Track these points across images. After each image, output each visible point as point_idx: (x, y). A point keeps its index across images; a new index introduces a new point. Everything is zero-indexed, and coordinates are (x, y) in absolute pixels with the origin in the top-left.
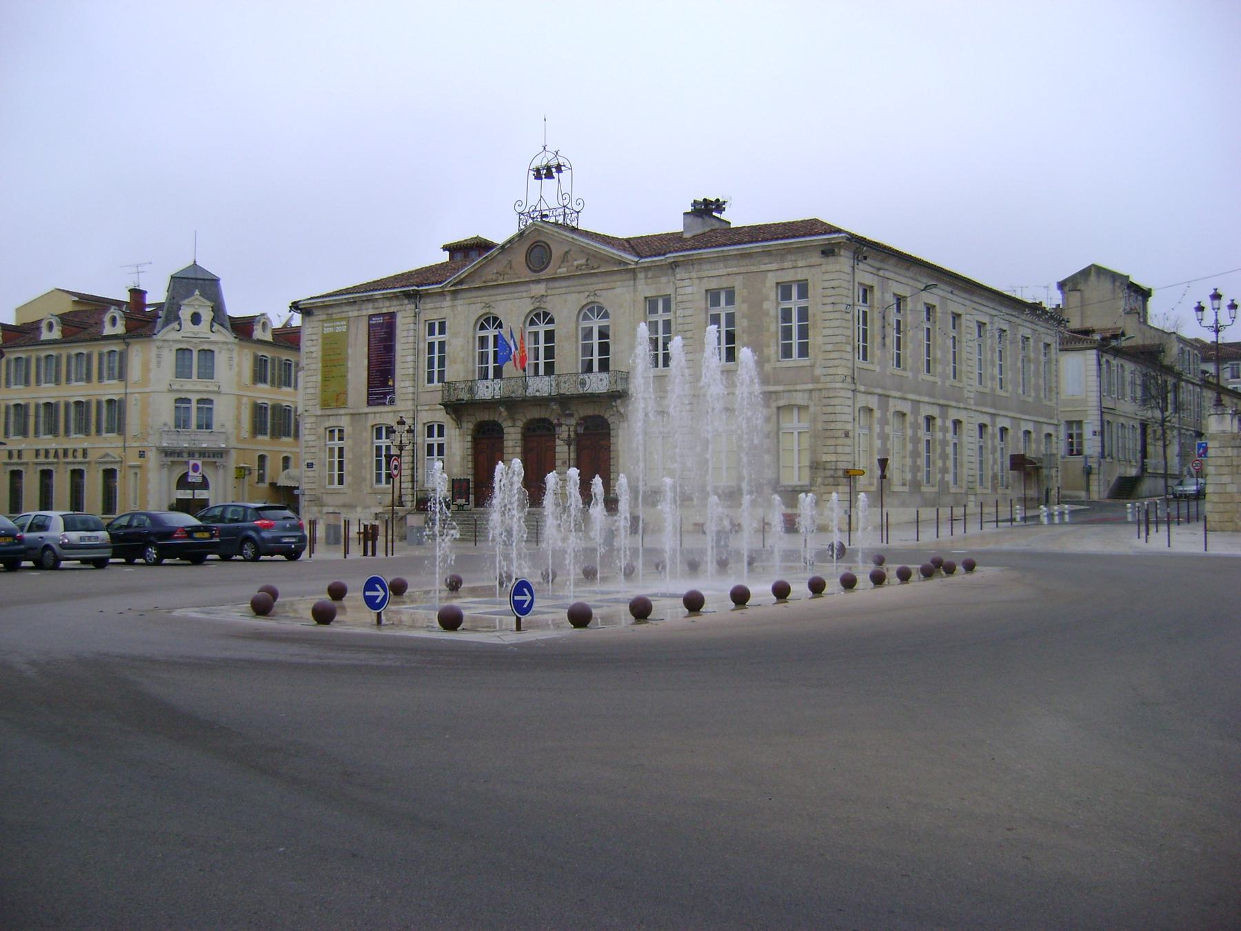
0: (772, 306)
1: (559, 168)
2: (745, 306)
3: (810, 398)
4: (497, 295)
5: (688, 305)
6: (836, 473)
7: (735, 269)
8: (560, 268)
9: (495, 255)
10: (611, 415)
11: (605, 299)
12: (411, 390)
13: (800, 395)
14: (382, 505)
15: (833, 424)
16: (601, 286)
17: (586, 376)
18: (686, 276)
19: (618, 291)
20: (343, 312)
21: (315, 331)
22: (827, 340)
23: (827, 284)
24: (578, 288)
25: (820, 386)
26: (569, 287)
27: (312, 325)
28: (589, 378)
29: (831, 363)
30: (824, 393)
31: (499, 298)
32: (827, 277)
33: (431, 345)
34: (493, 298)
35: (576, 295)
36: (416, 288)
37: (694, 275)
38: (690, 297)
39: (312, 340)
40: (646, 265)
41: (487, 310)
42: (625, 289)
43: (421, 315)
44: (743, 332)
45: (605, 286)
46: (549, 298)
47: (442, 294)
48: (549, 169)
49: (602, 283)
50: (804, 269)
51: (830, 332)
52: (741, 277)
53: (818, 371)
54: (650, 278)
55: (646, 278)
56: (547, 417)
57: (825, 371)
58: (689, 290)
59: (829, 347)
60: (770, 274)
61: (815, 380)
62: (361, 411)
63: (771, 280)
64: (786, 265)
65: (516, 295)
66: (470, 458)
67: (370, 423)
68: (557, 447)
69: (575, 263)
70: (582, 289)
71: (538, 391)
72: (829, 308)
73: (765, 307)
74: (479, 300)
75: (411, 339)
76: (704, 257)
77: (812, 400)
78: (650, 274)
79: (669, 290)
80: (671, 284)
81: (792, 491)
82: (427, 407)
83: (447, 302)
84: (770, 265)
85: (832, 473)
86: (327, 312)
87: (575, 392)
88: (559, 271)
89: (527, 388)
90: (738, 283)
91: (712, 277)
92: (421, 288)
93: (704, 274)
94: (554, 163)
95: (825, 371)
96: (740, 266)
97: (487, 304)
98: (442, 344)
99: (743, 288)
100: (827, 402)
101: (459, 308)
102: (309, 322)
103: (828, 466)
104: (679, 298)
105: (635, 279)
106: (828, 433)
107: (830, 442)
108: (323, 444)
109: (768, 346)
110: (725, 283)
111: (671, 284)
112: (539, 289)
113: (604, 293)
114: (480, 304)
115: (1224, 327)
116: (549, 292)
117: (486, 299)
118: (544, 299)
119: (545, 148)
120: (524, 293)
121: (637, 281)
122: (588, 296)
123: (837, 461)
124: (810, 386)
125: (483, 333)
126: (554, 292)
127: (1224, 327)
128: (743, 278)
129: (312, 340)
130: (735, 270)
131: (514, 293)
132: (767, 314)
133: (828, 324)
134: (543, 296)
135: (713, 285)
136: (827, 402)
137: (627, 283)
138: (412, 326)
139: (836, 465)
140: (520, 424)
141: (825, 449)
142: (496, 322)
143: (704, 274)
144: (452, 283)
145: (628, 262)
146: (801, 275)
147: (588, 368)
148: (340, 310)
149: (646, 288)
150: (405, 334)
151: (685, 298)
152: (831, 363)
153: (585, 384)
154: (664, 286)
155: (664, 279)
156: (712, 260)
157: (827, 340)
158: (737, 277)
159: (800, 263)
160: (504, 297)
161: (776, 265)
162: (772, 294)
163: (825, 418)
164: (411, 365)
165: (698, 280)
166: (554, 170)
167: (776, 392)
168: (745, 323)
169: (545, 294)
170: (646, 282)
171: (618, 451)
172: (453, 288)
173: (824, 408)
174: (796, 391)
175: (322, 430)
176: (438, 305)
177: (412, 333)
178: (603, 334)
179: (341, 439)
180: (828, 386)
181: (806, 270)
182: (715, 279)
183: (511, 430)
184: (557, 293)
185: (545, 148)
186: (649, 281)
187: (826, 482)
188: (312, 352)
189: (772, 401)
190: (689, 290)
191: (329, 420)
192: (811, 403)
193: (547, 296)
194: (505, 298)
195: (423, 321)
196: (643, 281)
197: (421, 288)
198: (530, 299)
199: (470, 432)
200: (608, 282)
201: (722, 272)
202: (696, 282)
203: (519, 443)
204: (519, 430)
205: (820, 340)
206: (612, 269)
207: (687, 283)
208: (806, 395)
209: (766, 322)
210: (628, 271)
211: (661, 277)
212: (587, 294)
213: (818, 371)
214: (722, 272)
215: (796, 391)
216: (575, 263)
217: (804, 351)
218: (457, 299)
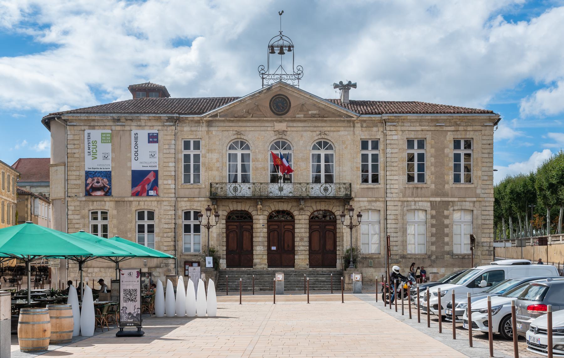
0: (450, 151)
1: (290, 48)
2: (433, 150)
3: (474, 206)
4: (247, 126)
5: (395, 146)
6: (490, 248)
7: (427, 127)
8: (298, 114)
9: (246, 100)
10: (337, 210)
11: (332, 137)
12: (173, 186)
13: (468, 204)
14: (148, 267)
15: (488, 221)
16: (329, 129)
17: (328, 185)
18: (392, 128)
19: (342, 133)
20: (106, 126)
21: (77, 137)
22: (486, 173)
23: (485, 142)
24: (311, 129)
25: (480, 199)
26: (304, 127)
27: (73, 132)
28: (330, 186)
29: (486, 187)
30: (484, 204)
31: (248, 129)
32: (484, 137)
33: (187, 157)
34: (243, 129)
35: (311, 133)
36: (178, 115)
37: (399, 128)
38: (396, 142)
39: (74, 144)
40: (365, 119)
41: (239, 136)
42: (346, 133)
43: (179, 134)
44: (431, 166)
45: (332, 129)
46: (288, 133)
47: (198, 122)
48: (282, 47)
49: (330, 127)
50: (471, 132)
51: (484, 169)
52: (430, 133)
53: (479, 191)
54: (365, 127)
55: (362, 127)
56: (288, 209)
57: (483, 191)
58: (395, 137)
59: (486, 178)
60: (449, 133)
61: (477, 196)
62: (126, 199)
63: (450, 137)
64: (461, 128)
65: (262, 128)
66: (225, 235)
67: (134, 209)
68: (296, 229)
69: (310, 112)
70: (315, 129)
71: (291, 192)
72: (486, 156)
73: (446, 151)
74: (231, 129)
75: (173, 151)
76: (408, 118)
77: (476, 207)
78: (365, 125)
79: (379, 136)
80: (380, 132)
81: (463, 258)
82: (186, 199)
83: (203, 128)
84: (450, 128)
85: (488, 248)
86: (89, 125)
87: (321, 195)
88: (297, 116)
89: (282, 191)
90: (429, 136)
91: (411, 131)
92: (181, 116)
93: (403, 128)
94: (286, 43)
95: (483, 191)
96: (431, 126)
97: (238, 132)
98: (197, 157)
99: (432, 139)
100: (484, 208)
101: (214, 133)
102: (70, 130)
103: (485, 244)
104: (388, 142)
105: (354, 127)
106: (486, 226)
107: (488, 231)
108: (88, 222)
109: (448, 175)
110: (420, 136)
111: (380, 132)
112: (281, 126)
113: (331, 134)
114: (232, 132)
115: (213, 226)
116: (289, 129)
117: (236, 129)
118: (285, 133)
119: (281, 33)
120: (269, 128)
121: (356, 128)
122: (320, 134)
123: (490, 242)
124: (475, 199)
125: (232, 152)
126: (293, 129)
127: (213, 226)
128: (432, 134)
129: (74, 144)
130: (427, 128)
131: (261, 127)
132: (447, 156)
133: (485, 164)
134: (284, 131)
135: (412, 136)
136: (484, 208)
137: (348, 129)
138: (173, 142)
139: (490, 244)
140: (266, 213)
141: (484, 235)
142: (243, 145)
143: (407, 128)
144: (210, 115)
145: (352, 115)
146: (469, 136)
147: (317, 180)
148: (103, 124)
149: (361, 134)
150: (167, 147)
151: (392, 142)
152: (486, 187)
153: (328, 190)
154: (376, 133)
155: (375, 129)
156: (412, 120)
157: (483, 173)
158: (428, 133)
159: (469, 128)
160: (253, 129)
161: (454, 127)
162: (452, 145)
163: (483, 217)
164: (173, 169)
165: (401, 132)
166: (284, 48)
167: (452, 202)
168: (433, 160)
169: (286, 130)
170: (362, 129)
171: (343, 233)
172: (210, 119)
173: (482, 212)
174: (465, 201)
175: (85, 212)
176: (193, 129)
177: (173, 147)
178: (328, 158)
179: (105, 218)
180: (486, 199)
181: (472, 133)
182: (413, 132)
183: (261, 217)
184: (295, 130)
185: (281, 33)
186: (364, 129)
187: (484, 254)
188: (74, 153)
189: (450, 207)
190: (395, 137)
191: (93, 205)
192: (474, 209)
193: (287, 131)
194: (253, 130)
195: (180, 139)
196: (360, 129)
197: (181, 116)
198: (273, 132)
199: (225, 217)
200: (334, 127)
201: (419, 128)
202: (400, 133)
203: (266, 226)
204: (266, 217)
205: (480, 173)
206: (340, 119)
207: (393, 133)
208: (472, 204)
209: (447, 161)
210: (349, 121)
211: (372, 127)
212: (318, 133)
213: (479, 191)
214: (419, 128)
215: (465, 201)
216: (310, 112)
217: (469, 180)
218: (212, 126)
